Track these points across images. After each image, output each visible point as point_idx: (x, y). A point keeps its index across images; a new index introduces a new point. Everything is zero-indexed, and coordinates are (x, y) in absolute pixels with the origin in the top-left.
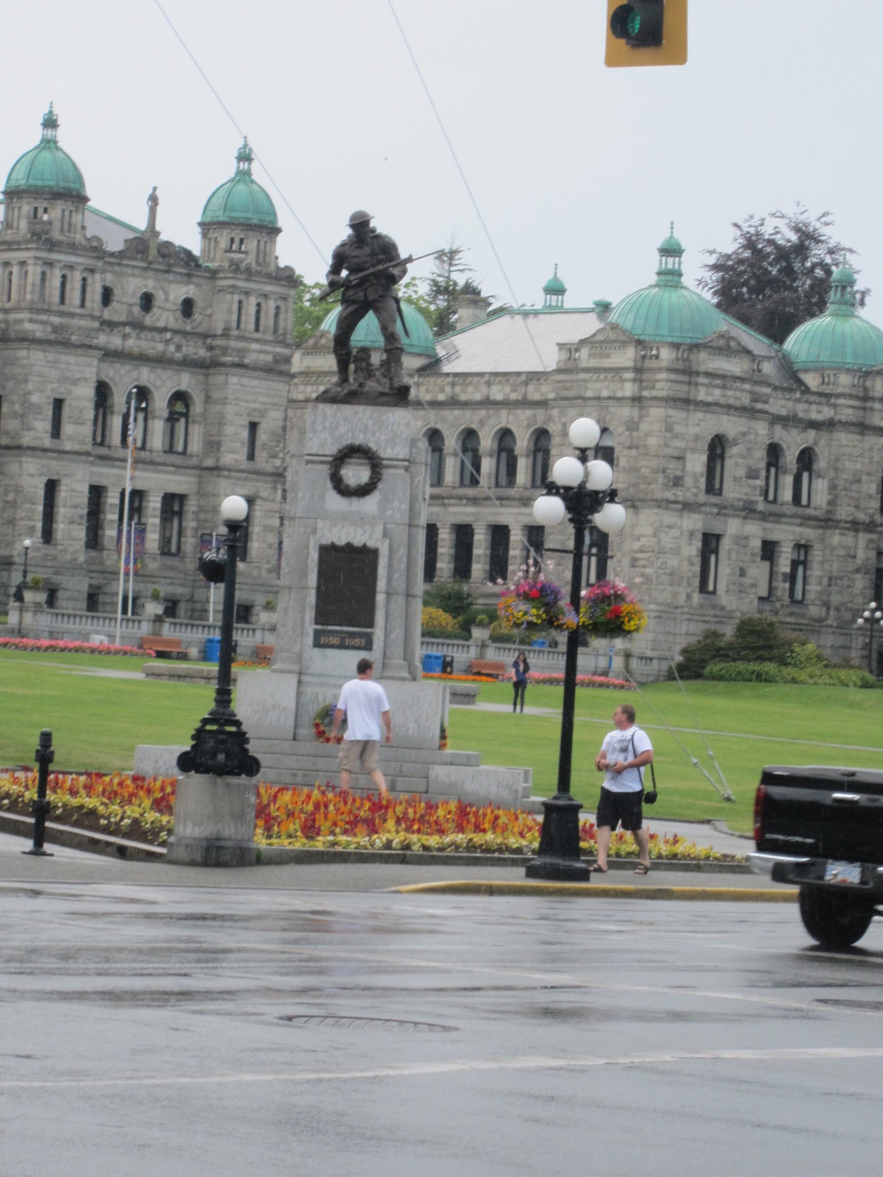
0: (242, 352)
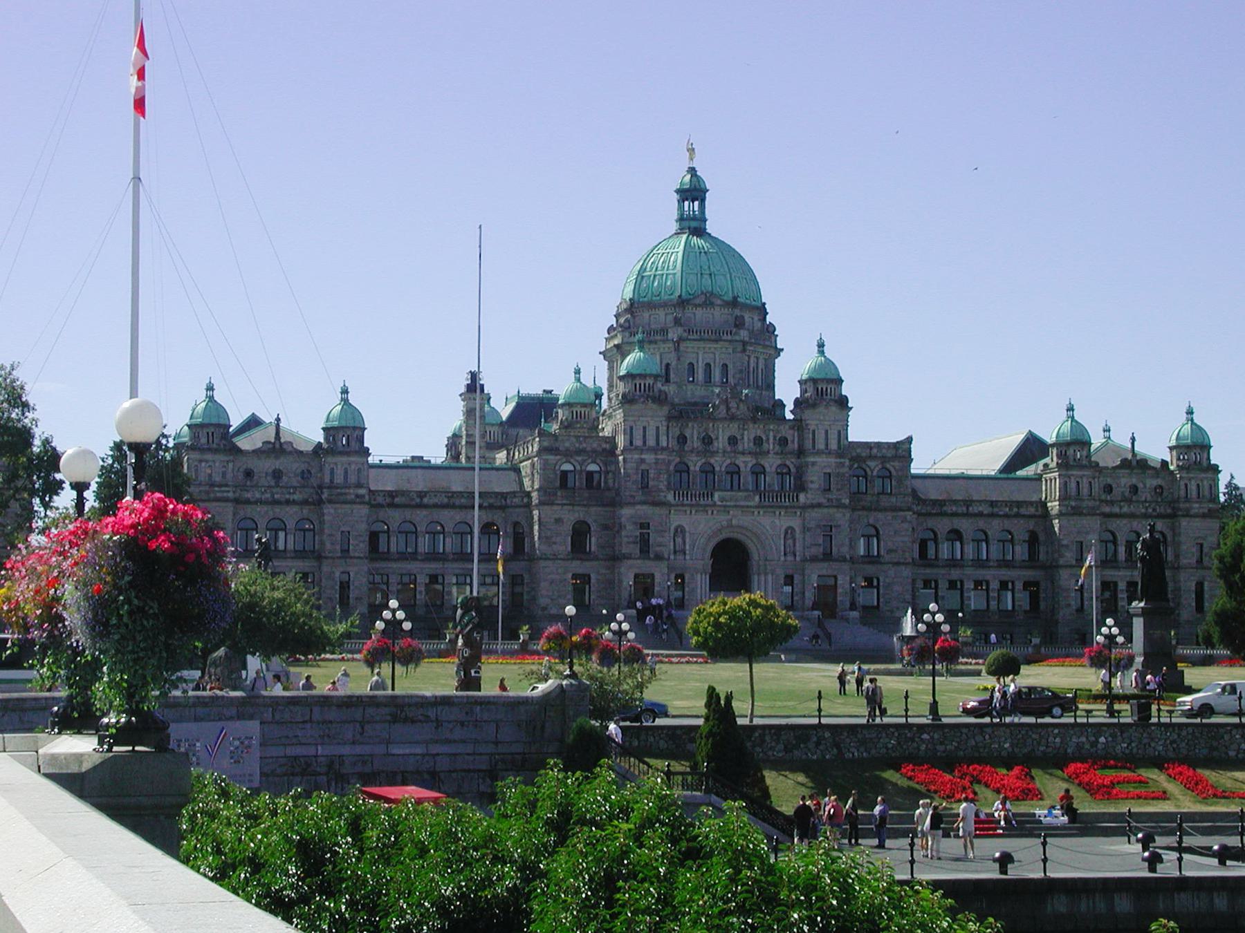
0: (1188, 510)
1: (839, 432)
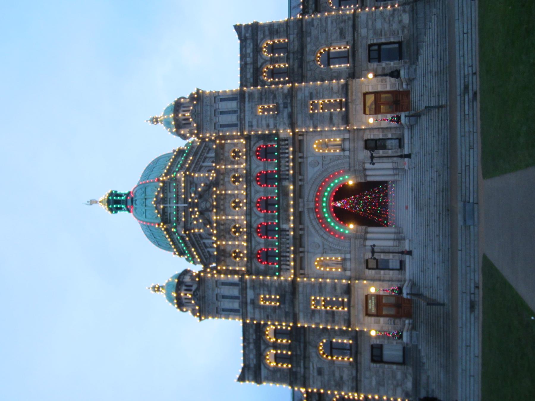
1: (222, 100)
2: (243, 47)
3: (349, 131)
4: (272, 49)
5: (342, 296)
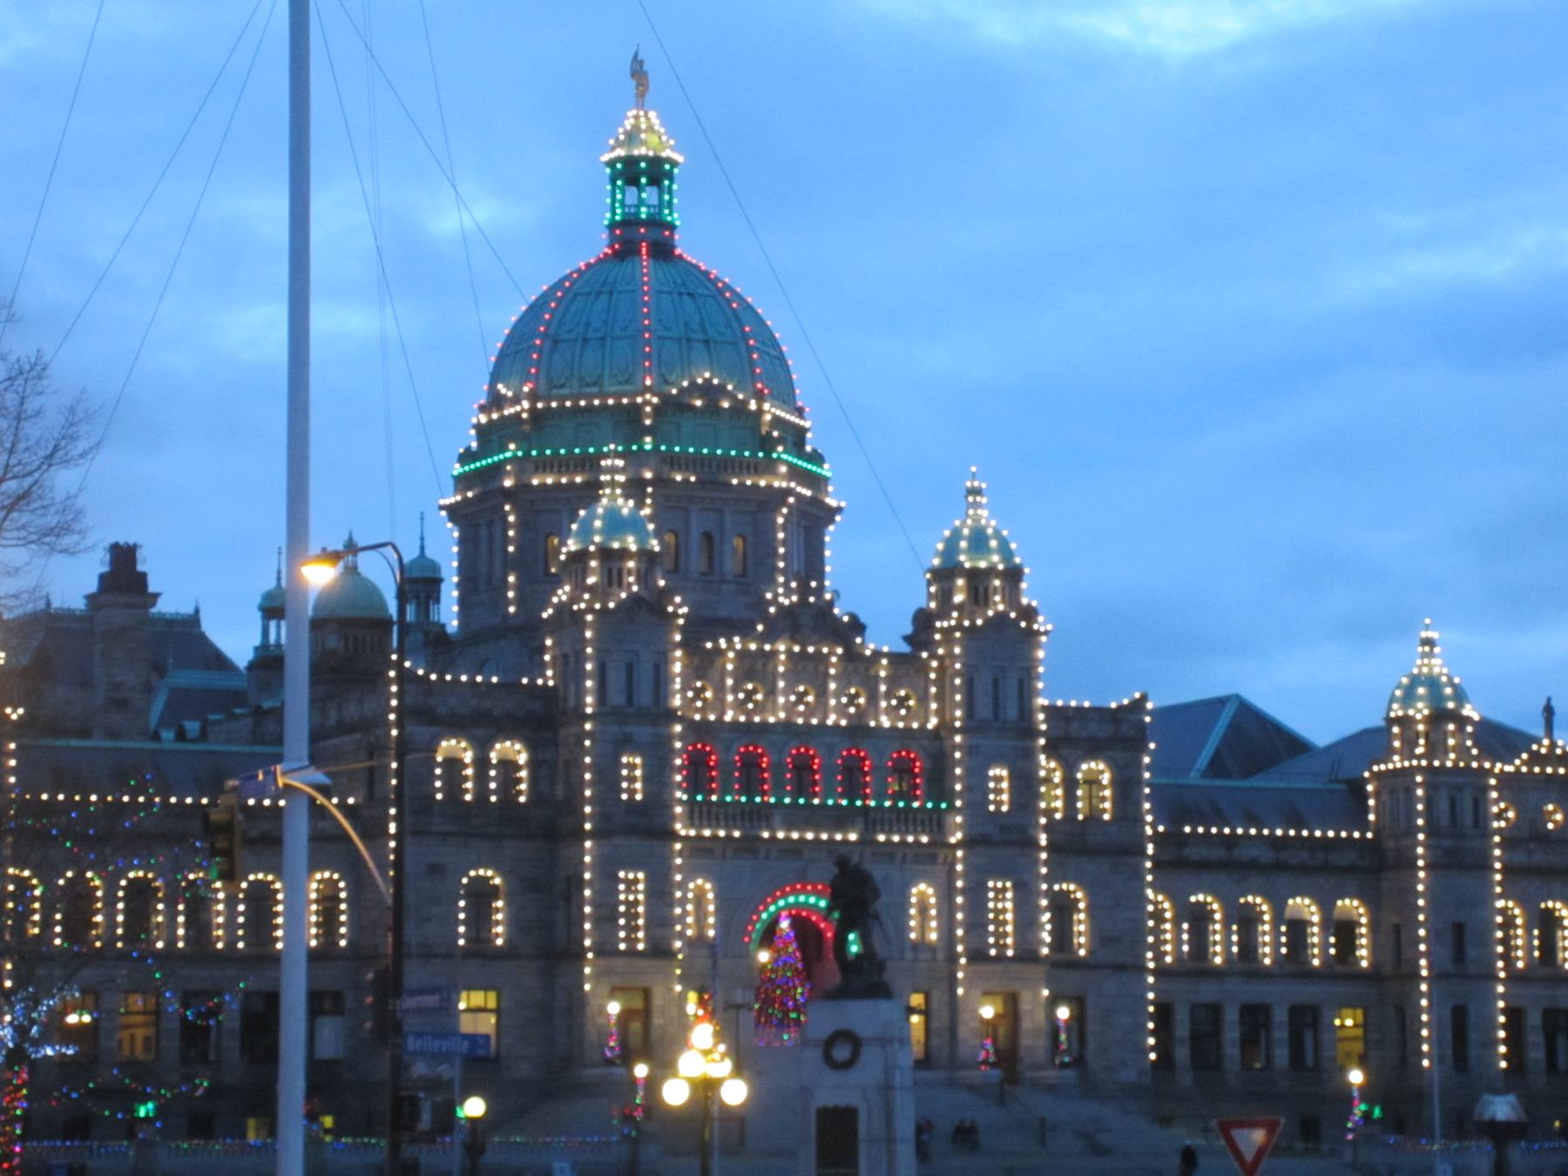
2: (1100, 713)
3: (953, 958)
4: (1093, 782)
5: (647, 939)
